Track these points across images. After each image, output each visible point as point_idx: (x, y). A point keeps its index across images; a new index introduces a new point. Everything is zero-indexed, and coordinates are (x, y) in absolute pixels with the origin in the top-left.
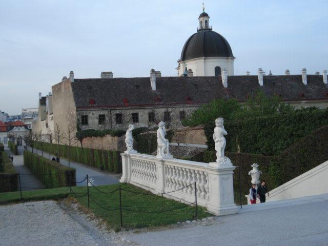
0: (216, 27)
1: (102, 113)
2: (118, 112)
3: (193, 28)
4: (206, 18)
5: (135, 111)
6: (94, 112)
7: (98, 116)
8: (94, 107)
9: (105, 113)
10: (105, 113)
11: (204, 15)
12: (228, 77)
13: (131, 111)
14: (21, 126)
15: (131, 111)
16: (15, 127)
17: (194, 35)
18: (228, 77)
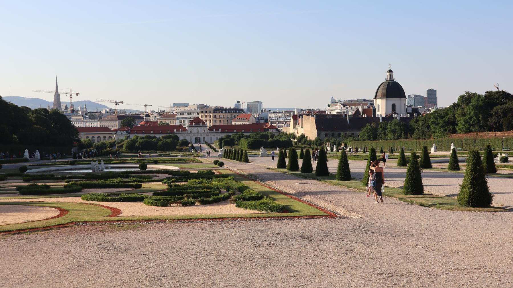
0: (397, 79)
1: (327, 133)
2: (333, 133)
3: (384, 78)
4: (391, 73)
5: (340, 133)
6: (323, 132)
7: (325, 134)
8: (323, 131)
9: (328, 133)
10: (328, 133)
11: (390, 71)
12: (436, 90)
13: (338, 133)
14: (274, 129)
15: (338, 133)
16: (270, 130)
17: (383, 83)
18: (436, 90)
